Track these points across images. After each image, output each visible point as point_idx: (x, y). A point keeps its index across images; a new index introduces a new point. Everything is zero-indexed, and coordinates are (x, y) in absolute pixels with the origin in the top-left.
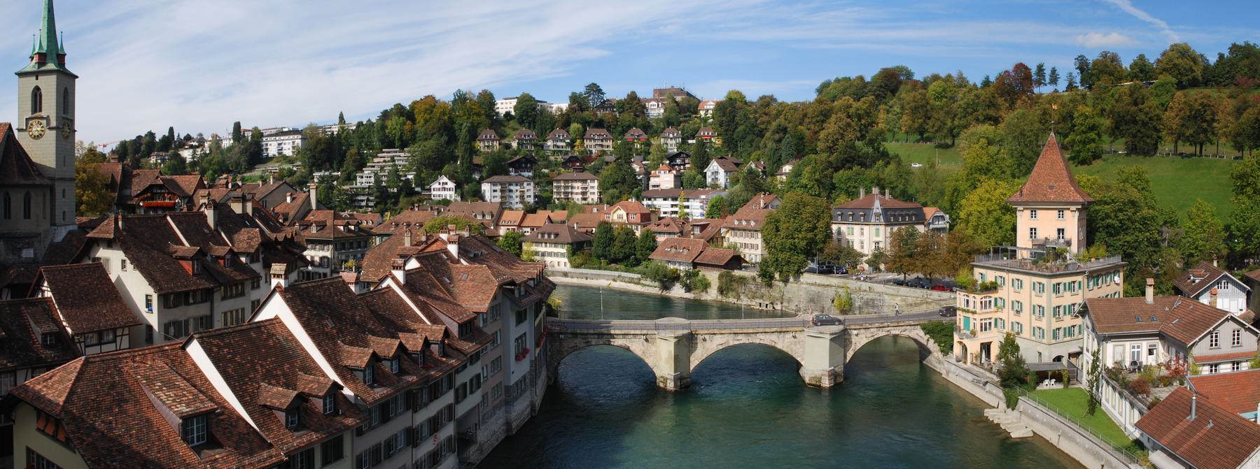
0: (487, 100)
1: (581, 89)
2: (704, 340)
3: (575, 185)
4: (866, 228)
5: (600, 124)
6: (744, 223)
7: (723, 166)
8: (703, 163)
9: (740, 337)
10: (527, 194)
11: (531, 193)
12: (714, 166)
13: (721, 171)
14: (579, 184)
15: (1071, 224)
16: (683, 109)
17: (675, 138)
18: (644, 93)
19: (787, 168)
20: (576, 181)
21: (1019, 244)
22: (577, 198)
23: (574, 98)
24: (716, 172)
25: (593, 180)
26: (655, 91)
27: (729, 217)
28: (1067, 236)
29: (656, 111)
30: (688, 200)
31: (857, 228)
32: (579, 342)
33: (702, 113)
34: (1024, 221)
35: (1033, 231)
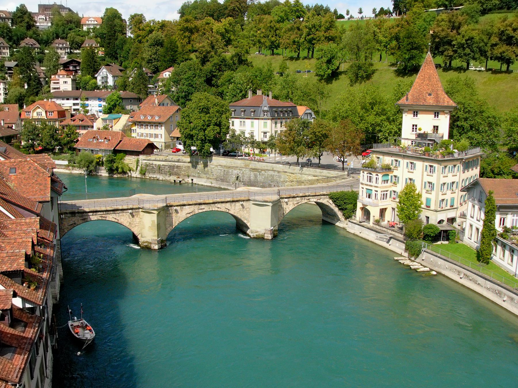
2: (176, 211)
6: (149, 118)
7: (110, 71)
8: (94, 70)
9: (203, 206)
12: (104, 71)
15: (444, 122)
16: (68, 24)
17: (65, 48)
18: (33, 8)
21: (403, 136)
28: (440, 131)
29: (43, 23)
30: (87, 99)
32: (75, 219)
33: (85, 28)
34: (408, 120)
35: (414, 126)
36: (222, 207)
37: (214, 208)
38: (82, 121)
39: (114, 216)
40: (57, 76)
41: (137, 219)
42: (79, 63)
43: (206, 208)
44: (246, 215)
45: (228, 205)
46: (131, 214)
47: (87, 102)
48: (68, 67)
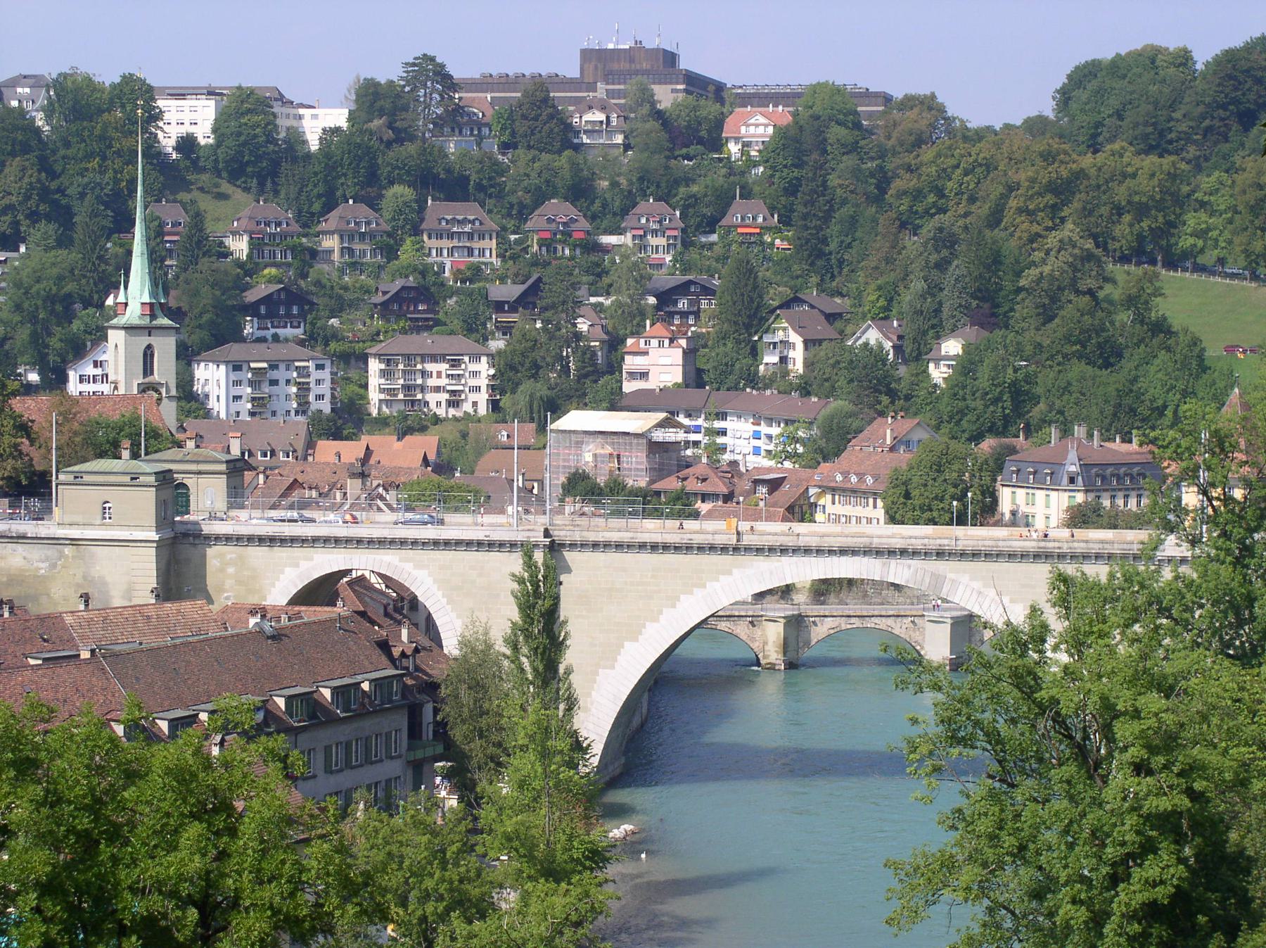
0: (137, 100)
1: (389, 71)
3: (430, 367)
4: (1054, 494)
5: (454, 187)
6: (854, 479)
9: (853, 620)
10: (315, 390)
11: (325, 388)
13: (796, 338)
14: (443, 367)
19: (952, 347)
20: (434, 358)
22: (436, 403)
23: (372, 98)
24: (788, 348)
25: (476, 357)
26: (586, 55)
27: (825, 467)
30: (722, 416)
31: (1040, 495)
33: (734, 148)
36: (883, 623)
37: (869, 623)
38: (704, 480)
39: (728, 624)
40: (642, 341)
41: (758, 632)
42: (708, 291)
43: (857, 623)
44: (919, 639)
45: (890, 621)
46: (751, 622)
47: (718, 424)
48: (675, 303)
